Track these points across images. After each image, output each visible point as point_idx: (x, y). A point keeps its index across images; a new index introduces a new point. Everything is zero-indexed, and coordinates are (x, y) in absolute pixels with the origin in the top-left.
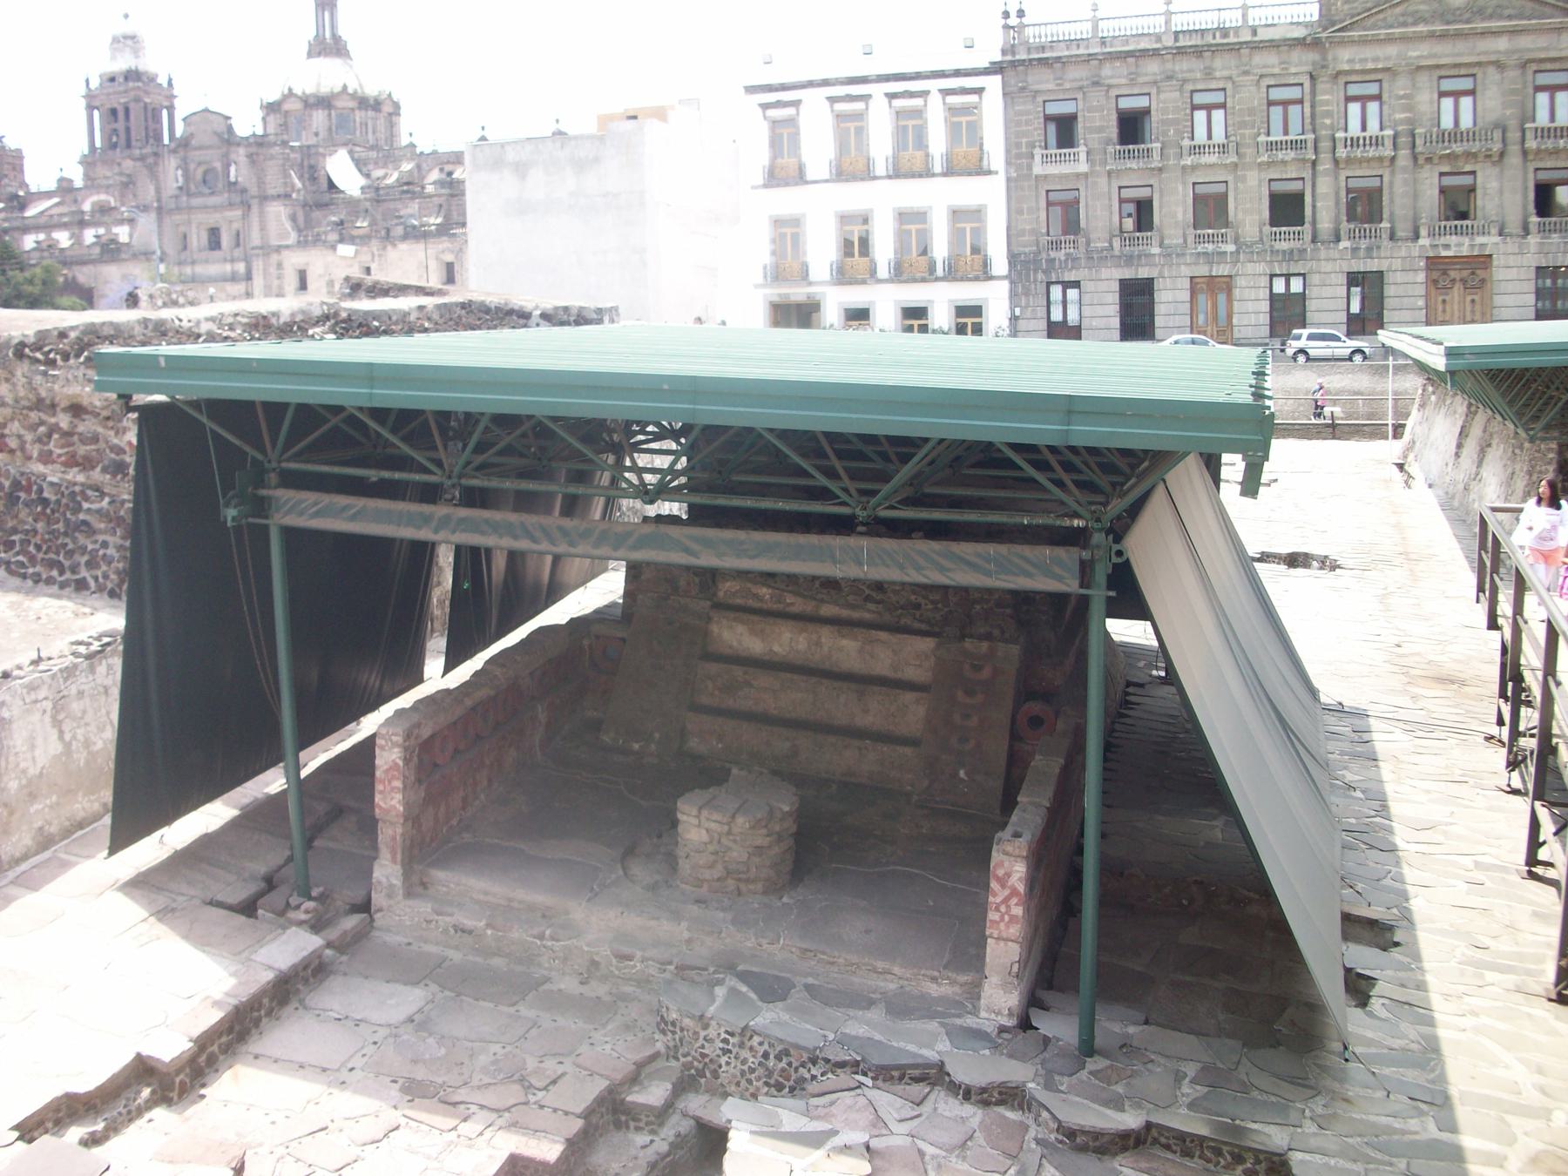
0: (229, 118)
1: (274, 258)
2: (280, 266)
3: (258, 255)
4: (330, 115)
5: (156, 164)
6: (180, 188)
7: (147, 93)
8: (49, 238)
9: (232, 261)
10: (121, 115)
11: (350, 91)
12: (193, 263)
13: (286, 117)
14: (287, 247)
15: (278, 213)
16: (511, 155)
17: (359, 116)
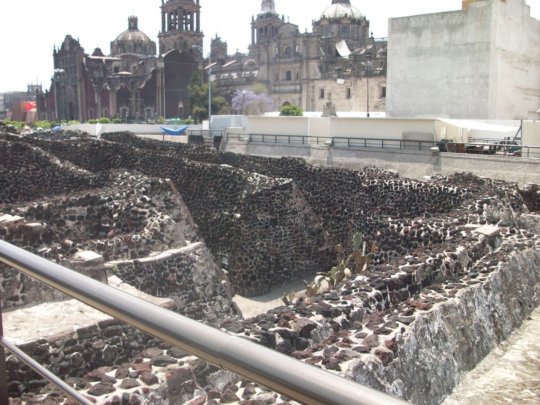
0: (298, 26)
1: (311, 84)
2: (313, 87)
3: (305, 83)
4: (339, 26)
5: (268, 45)
6: (277, 55)
7: (274, 22)
8: (230, 75)
9: (295, 85)
10: (264, 31)
11: (348, 16)
12: (280, 85)
13: (322, 27)
14: (317, 79)
15: (314, 65)
16: (413, 24)
17: (351, 26)
